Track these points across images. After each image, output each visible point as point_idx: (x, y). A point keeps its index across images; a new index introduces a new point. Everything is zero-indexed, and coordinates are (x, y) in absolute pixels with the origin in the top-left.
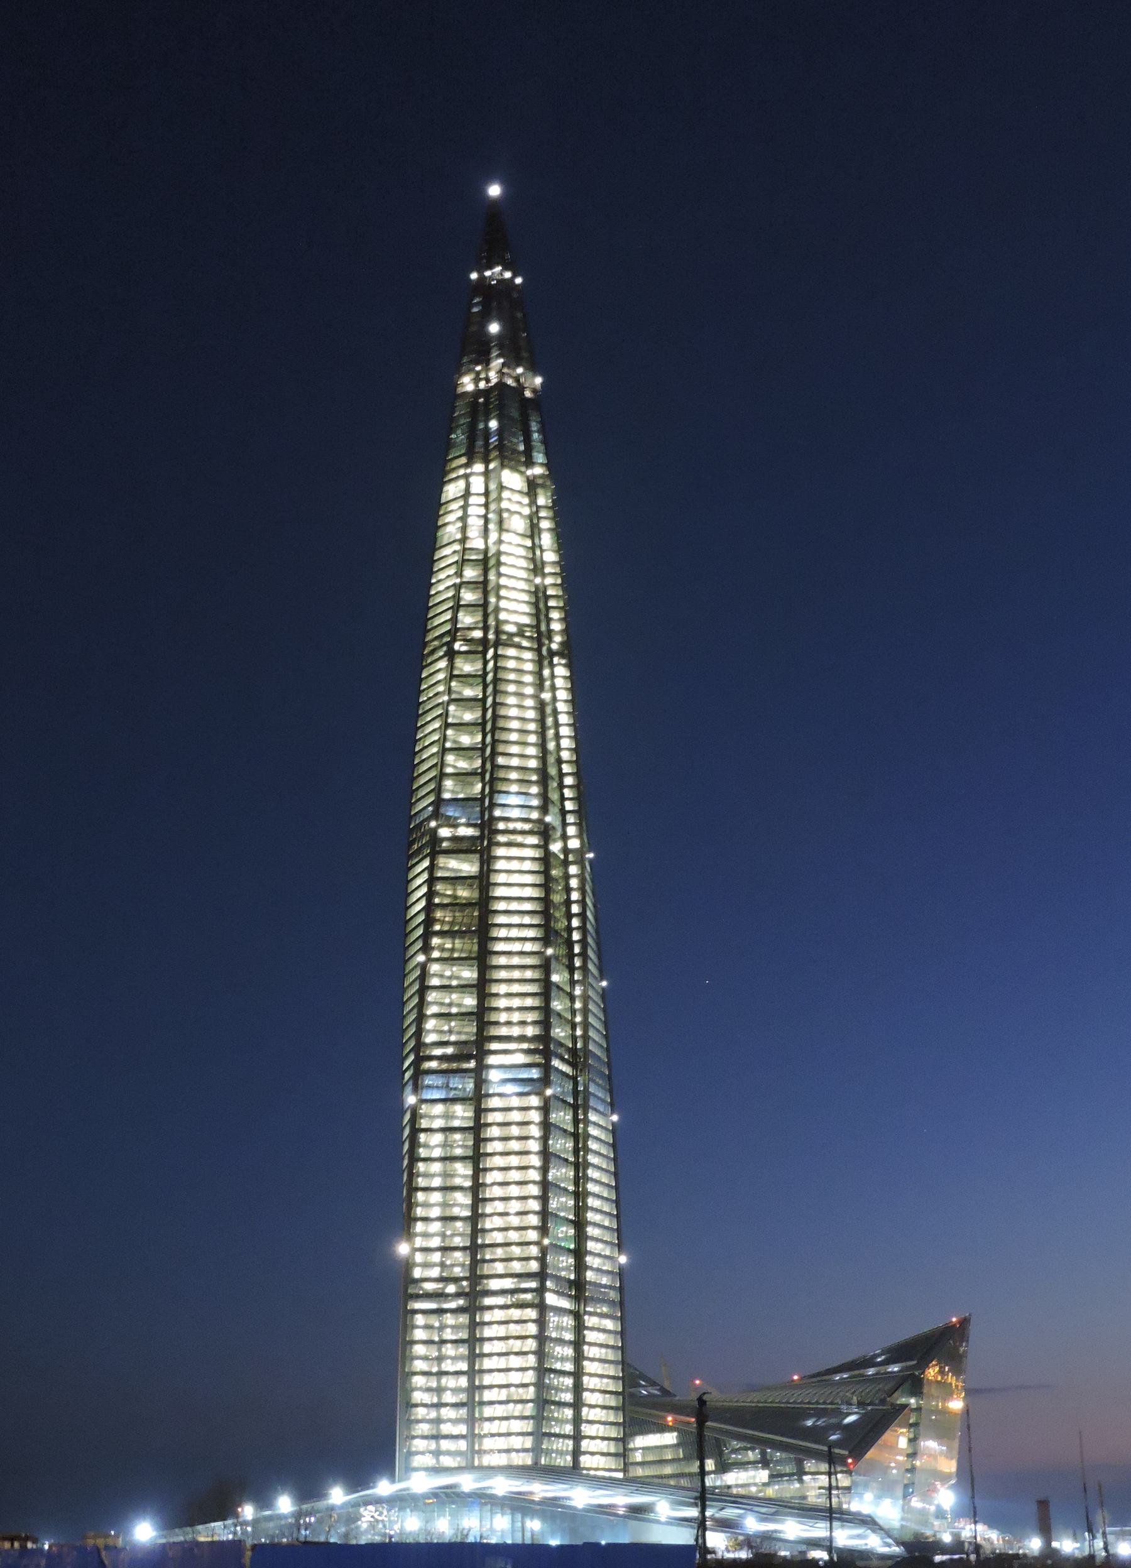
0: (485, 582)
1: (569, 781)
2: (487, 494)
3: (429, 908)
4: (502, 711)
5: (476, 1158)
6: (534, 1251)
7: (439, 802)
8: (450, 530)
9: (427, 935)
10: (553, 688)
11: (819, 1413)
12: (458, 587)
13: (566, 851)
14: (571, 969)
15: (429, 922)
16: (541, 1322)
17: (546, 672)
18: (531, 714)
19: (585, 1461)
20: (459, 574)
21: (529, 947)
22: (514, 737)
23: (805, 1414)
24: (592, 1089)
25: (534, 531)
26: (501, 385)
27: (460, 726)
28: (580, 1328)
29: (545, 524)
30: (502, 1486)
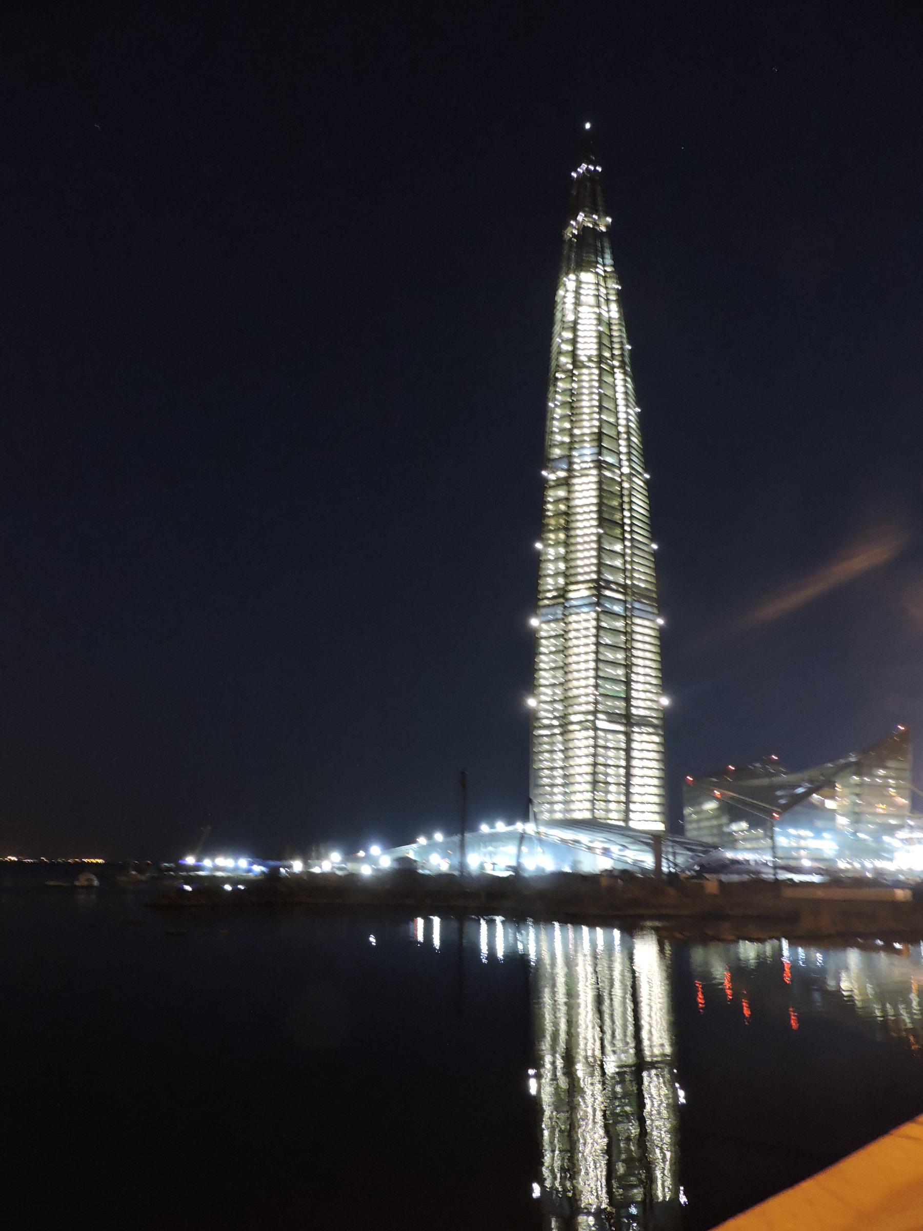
6: (591, 699)
16: (595, 738)
20: (560, 336)
21: (594, 530)
28: (629, 741)
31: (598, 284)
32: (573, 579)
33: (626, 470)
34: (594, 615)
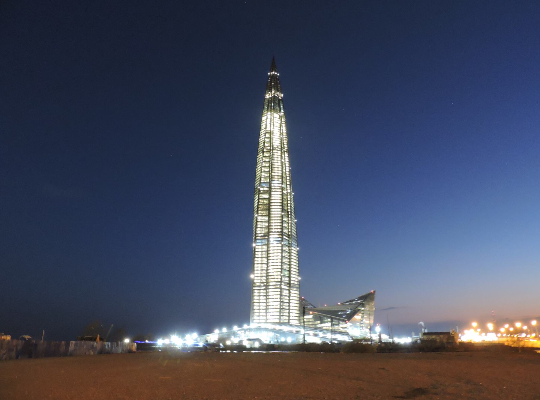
0: (270, 137)
1: (288, 178)
2: (271, 119)
3: (258, 204)
4: (274, 164)
5: (267, 257)
6: (279, 277)
7: (260, 183)
8: (263, 127)
9: (257, 211)
10: (285, 159)
11: (342, 311)
12: (265, 138)
13: (287, 193)
14: (288, 217)
15: (258, 208)
17: (283, 156)
18: (280, 164)
19: (291, 321)
22: (276, 169)
23: (339, 311)
24: (293, 242)
25: (281, 126)
26: (274, 96)
27: (265, 167)
28: (290, 293)
29: (284, 125)
30: (270, 326)
32: (271, 230)
33: (289, 191)
34: (280, 245)
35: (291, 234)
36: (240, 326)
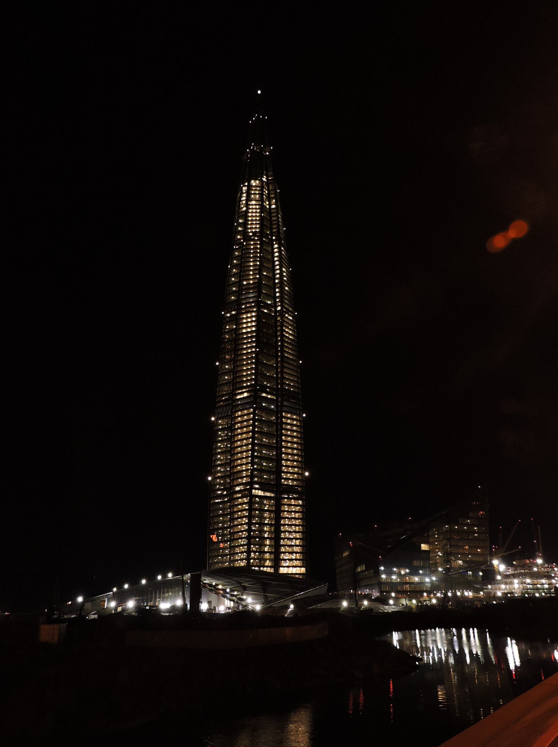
16: (250, 503)
31: (262, 187)
33: (279, 308)
35: (283, 388)
36: (151, 578)
